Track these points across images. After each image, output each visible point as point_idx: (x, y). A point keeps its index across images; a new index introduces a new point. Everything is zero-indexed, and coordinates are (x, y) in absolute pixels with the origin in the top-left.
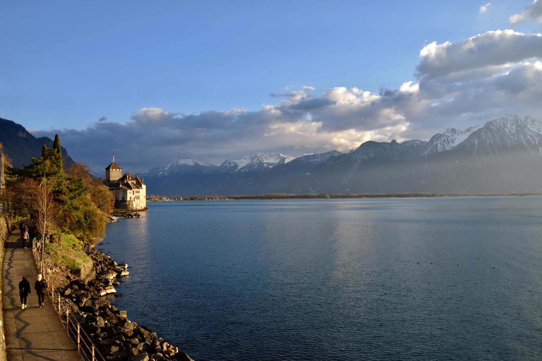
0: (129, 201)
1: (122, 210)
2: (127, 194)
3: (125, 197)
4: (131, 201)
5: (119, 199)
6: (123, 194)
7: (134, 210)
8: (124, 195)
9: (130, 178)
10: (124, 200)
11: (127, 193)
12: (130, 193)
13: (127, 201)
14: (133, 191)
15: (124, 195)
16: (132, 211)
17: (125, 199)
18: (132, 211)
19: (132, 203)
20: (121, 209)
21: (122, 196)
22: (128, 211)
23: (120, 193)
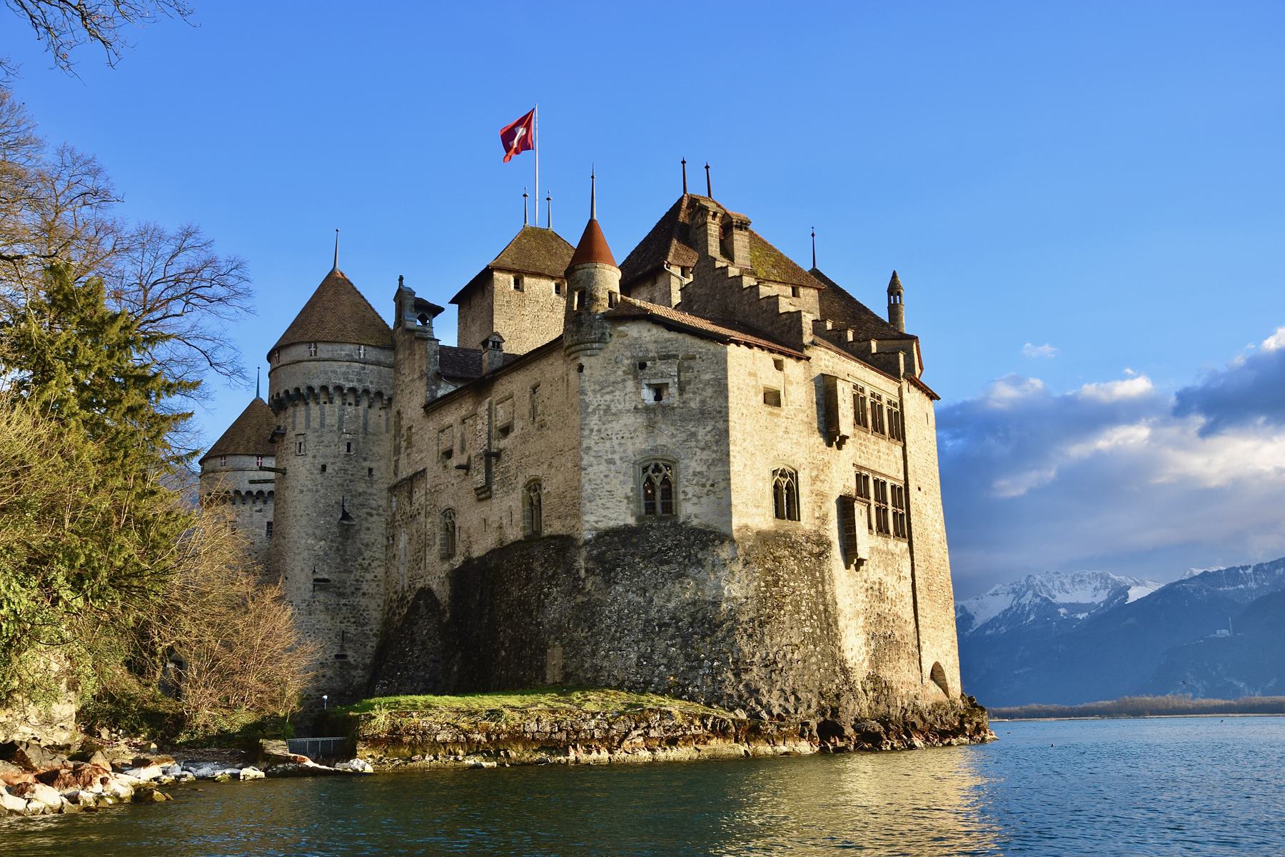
0: (764, 538)
1: (640, 717)
2: (723, 414)
3: (692, 464)
4: (792, 545)
5: (574, 508)
6: (655, 414)
7: (857, 707)
8: (667, 437)
9: (740, 241)
10: (678, 527)
11: (722, 388)
12: (773, 398)
13: (724, 537)
14: (826, 390)
15: (667, 437)
16: (830, 729)
17: (691, 509)
18: (830, 729)
19: (820, 582)
20: (618, 700)
21: (640, 444)
22: (753, 731)
23: (593, 400)
